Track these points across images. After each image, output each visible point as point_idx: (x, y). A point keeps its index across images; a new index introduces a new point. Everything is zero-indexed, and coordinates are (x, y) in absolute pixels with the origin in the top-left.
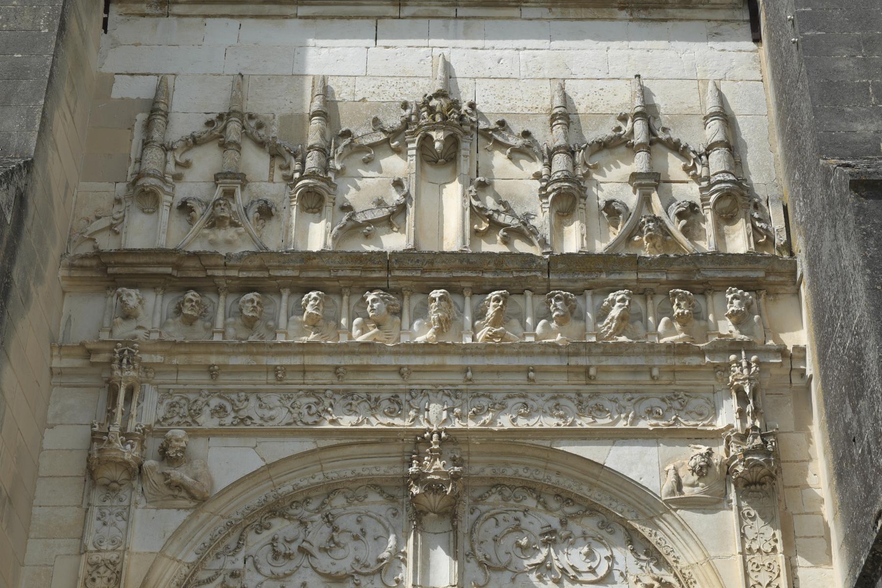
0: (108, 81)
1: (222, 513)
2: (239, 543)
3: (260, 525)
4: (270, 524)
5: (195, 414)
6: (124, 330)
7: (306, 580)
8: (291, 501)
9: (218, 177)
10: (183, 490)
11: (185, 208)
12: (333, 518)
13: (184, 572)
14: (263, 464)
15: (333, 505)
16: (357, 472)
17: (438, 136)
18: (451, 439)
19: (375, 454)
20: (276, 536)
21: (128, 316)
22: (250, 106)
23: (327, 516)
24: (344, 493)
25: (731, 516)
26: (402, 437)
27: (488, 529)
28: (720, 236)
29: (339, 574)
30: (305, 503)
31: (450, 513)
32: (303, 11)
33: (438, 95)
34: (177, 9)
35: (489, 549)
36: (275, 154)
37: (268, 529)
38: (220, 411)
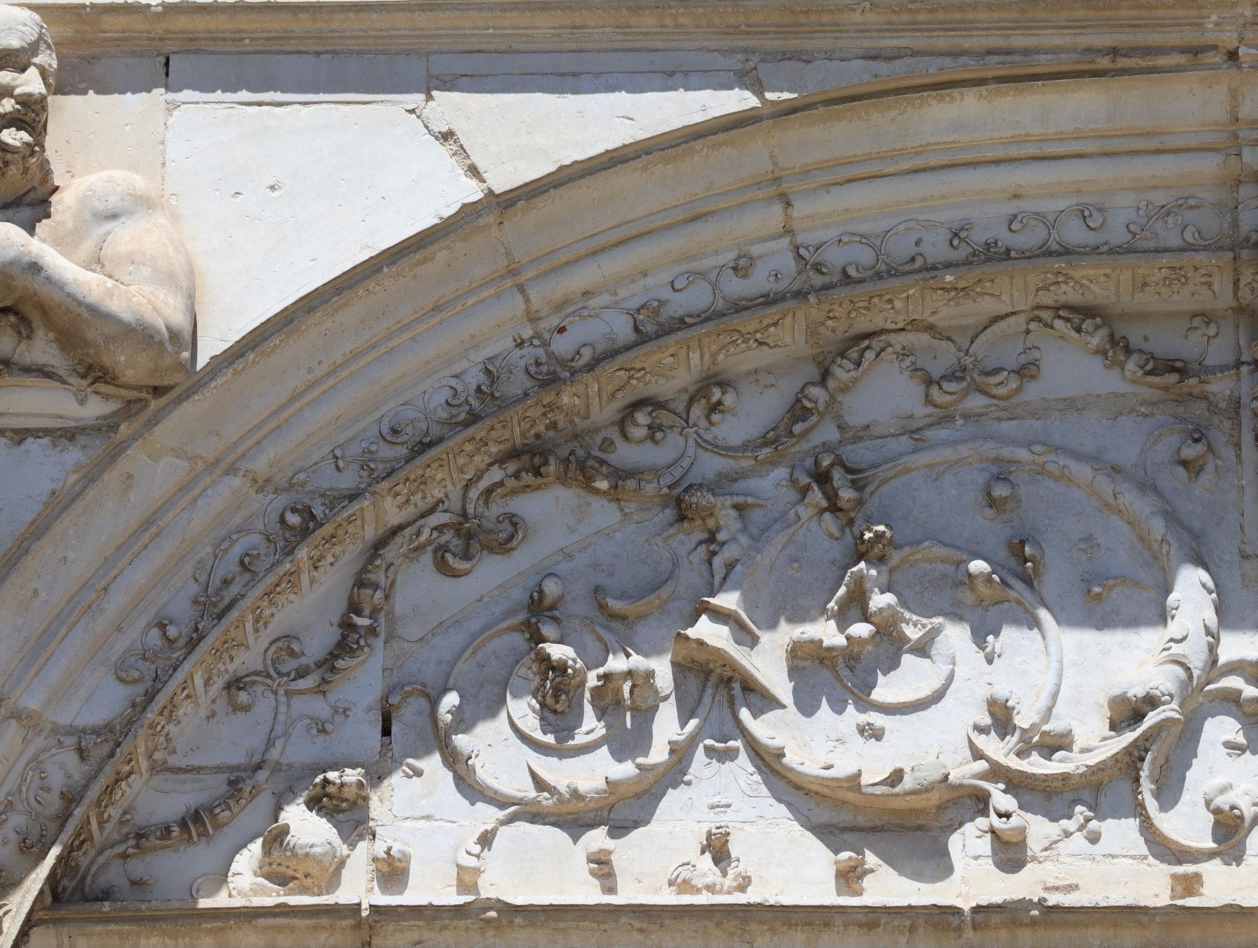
1: (260, 464)
2: (347, 626)
3: (457, 529)
4: (514, 521)
7: (725, 818)
8: (623, 399)
10: (40, 332)
12: (857, 486)
13: (56, 780)
14: (472, 192)
15: (855, 420)
16: (979, 237)
19: (1078, 136)
20: (552, 588)
23: (822, 478)
24: (905, 353)
26: (1228, 38)
29: (908, 783)
30: (697, 411)
37: (504, 547)
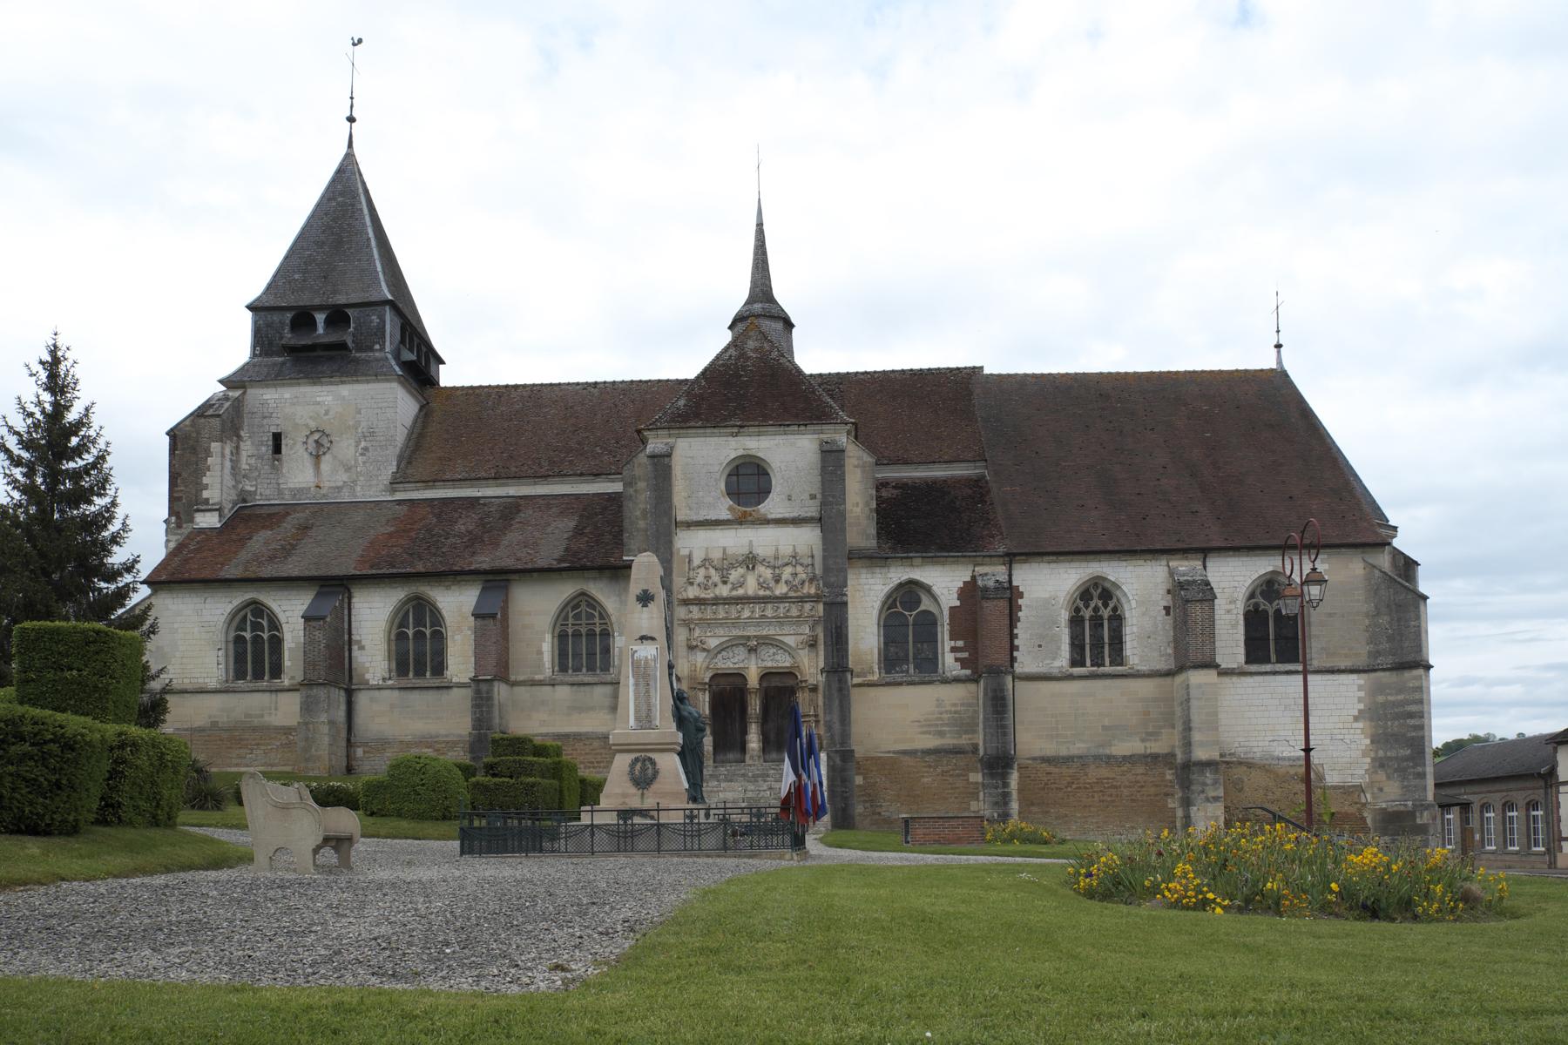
0: (679, 549)
5: (706, 632)
6: (690, 615)
9: (706, 577)
11: (699, 585)
17: (751, 566)
18: (755, 636)
21: (691, 612)
22: (711, 556)
25: (806, 650)
27: (763, 653)
28: (809, 588)
31: (756, 650)
32: (720, 527)
33: (751, 553)
34: (692, 528)
35: (762, 657)
36: (716, 569)
38: (710, 631)
